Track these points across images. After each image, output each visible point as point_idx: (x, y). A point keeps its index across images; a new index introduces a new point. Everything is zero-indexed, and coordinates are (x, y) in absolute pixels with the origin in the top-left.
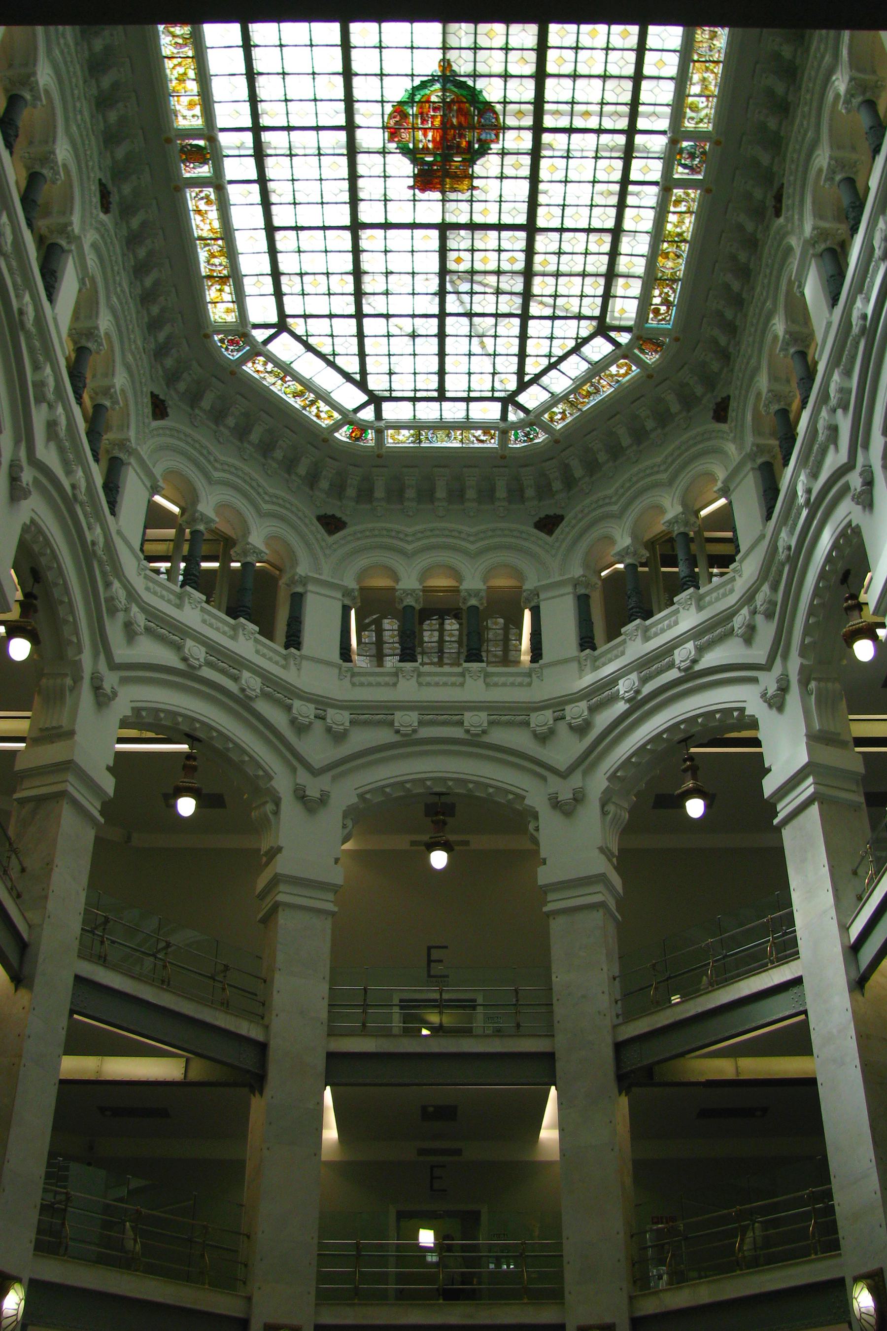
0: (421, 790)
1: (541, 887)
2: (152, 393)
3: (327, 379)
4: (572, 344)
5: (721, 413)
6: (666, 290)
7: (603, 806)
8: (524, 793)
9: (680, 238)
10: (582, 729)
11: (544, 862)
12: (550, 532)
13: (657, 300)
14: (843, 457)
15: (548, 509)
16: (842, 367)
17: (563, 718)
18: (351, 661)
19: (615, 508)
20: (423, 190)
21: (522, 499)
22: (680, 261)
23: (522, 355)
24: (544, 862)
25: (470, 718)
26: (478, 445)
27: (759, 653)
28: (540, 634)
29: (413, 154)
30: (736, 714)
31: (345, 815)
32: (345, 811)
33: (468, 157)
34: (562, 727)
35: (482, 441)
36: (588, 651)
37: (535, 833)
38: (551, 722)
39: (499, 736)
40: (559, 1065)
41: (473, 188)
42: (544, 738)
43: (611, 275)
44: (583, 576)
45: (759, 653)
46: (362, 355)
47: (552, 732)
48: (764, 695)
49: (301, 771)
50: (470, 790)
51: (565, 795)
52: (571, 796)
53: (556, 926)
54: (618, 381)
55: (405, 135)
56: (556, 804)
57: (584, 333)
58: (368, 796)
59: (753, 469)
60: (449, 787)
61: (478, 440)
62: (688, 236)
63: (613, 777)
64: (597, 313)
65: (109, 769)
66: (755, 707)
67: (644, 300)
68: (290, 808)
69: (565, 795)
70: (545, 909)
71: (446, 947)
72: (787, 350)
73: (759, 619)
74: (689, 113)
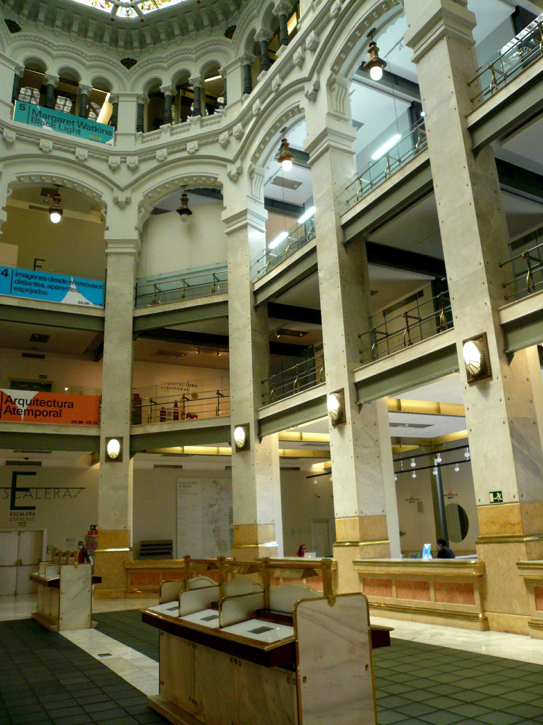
0: (49, 182)
1: (105, 240)
5: (229, 33)
7: (139, 208)
8: (101, 194)
10: (134, 170)
11: (108, 229)
12: (129, 68)
14: (305, 73)
15: (129, 55)
16: (316, 30)
17: (125, 162)
18: (53, 108)
19: (165, 65)
21: (117, 45)
24: (108, 229)
25: (78, 151)
26: (100, 8)
27: (230, 154)
28: (117, 118)
30: (212, 179)
31: (9, 185)
32: (9, 184)
34: (123, 166)
35: (102, 6)
36: (141, 132)
37: (104, 214)
38: (119, 163)
39: (91, 163)
40: (106, 324)
42: (114, 169)
44: (143, 95)
45: (230, 154)
47: (118, 168)
48: (229, 174)
50: (74, 187)
51: (122, 198)
52: (125, 200)
53: (111, 260)
56: (117, 202)
58: (22, 179)
59: (241, 66)
60: (65, 183)
63: (146, 196)
66: (223, 179)
70: (106, 251)
71: (44, 260)
72: (278, 12)
73: (233, 139)
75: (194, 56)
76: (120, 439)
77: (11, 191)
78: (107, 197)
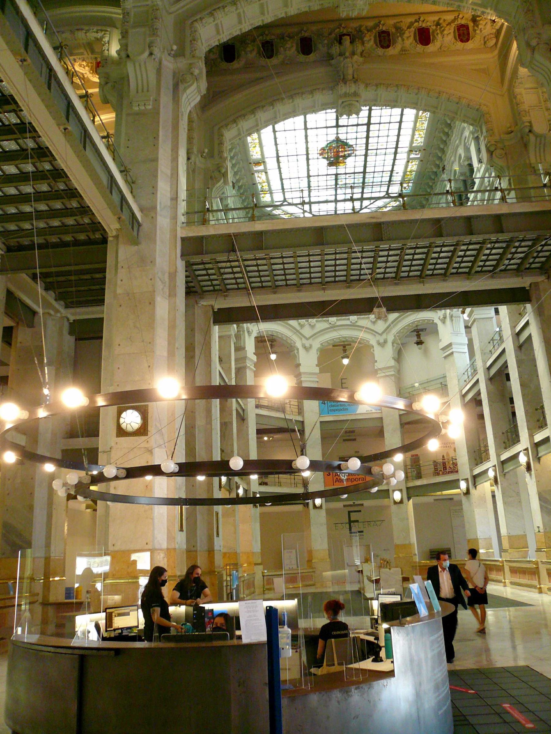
11: (376, 361)
20: (330, 166)
29: (327, 159)
31: (317, 350)
49: (303, 339)
56: (379, 344)
65: (254, 354)
66: (437, 321)
68: (302, 352)
69: (382, 341)
76: (401, 491)
77: (319, 353)
78: (373, 341)
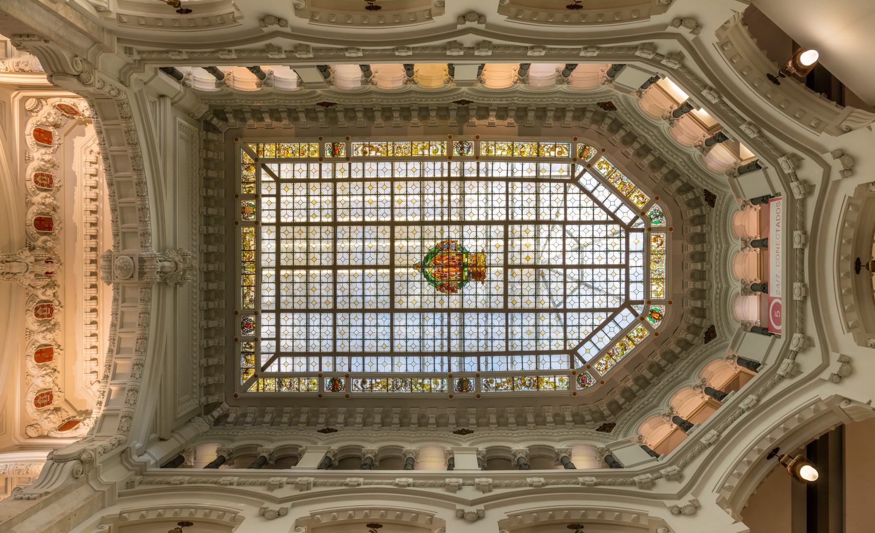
2: (597, 430)
3: (612, 330)
4: (584, 196)
6: (545, 150)
9: (512, 149)
13: (553, 154)
20: (485, 277)
22: (525, 145)
23: (593, 223)
26: (664, 245)
33: (464, 255)
41: (483, 252)
42: (808, 188)
43: (537, 180)
46: (593, 310)
54: (613, 168)
55: (453, 284)
57: (577, 190)
61: (661, 245)
62: (510, 144)
64: (562, 184)
67: (552, 160)
68: (846, 390)
74: (439, 153)
75: (655, 131)
